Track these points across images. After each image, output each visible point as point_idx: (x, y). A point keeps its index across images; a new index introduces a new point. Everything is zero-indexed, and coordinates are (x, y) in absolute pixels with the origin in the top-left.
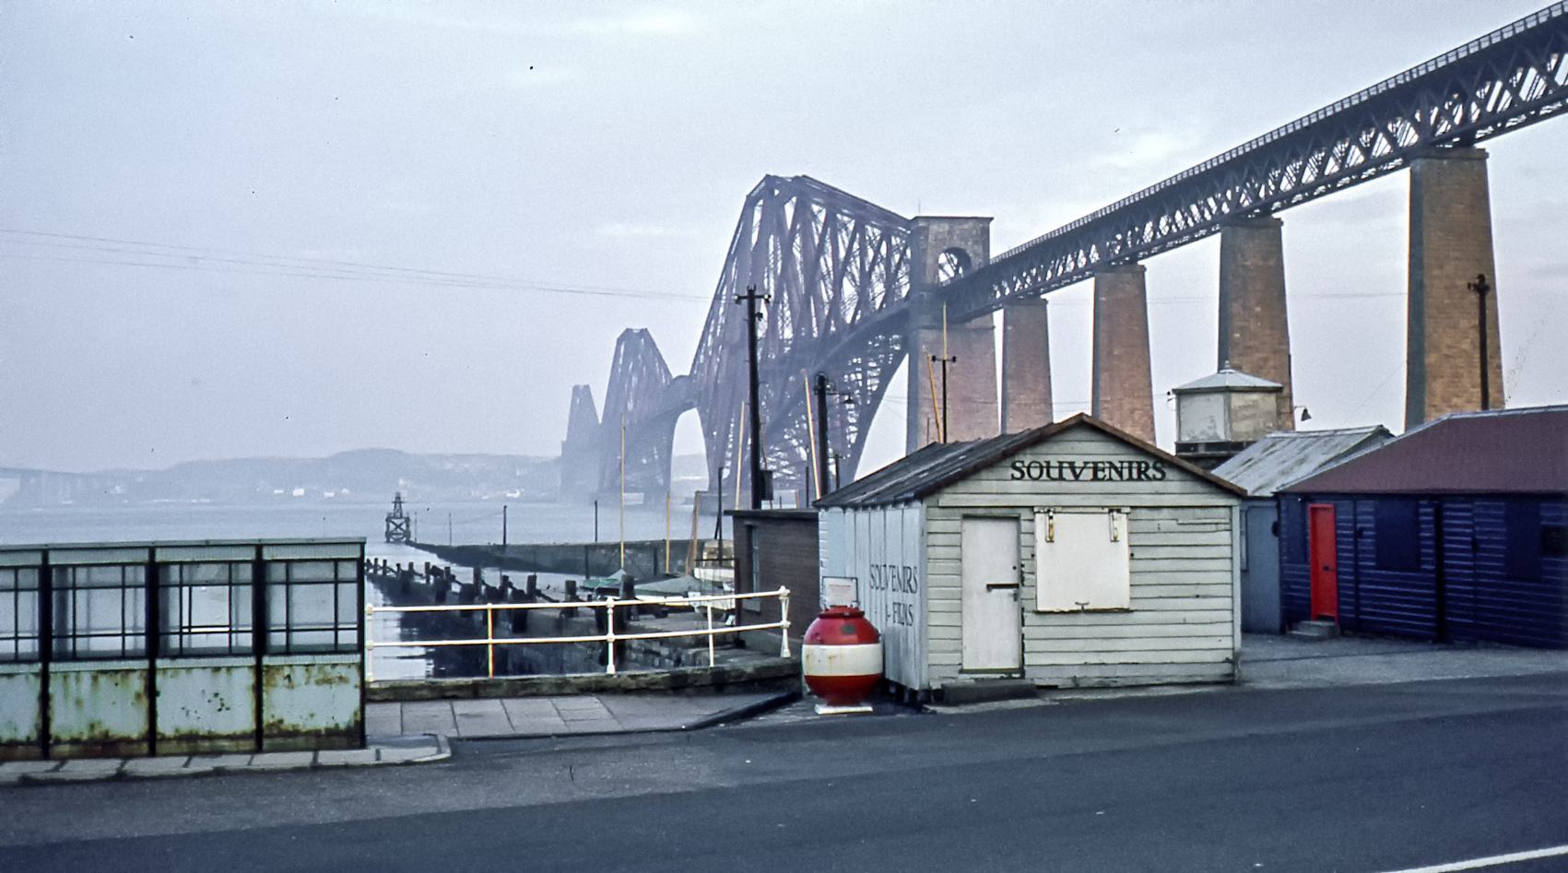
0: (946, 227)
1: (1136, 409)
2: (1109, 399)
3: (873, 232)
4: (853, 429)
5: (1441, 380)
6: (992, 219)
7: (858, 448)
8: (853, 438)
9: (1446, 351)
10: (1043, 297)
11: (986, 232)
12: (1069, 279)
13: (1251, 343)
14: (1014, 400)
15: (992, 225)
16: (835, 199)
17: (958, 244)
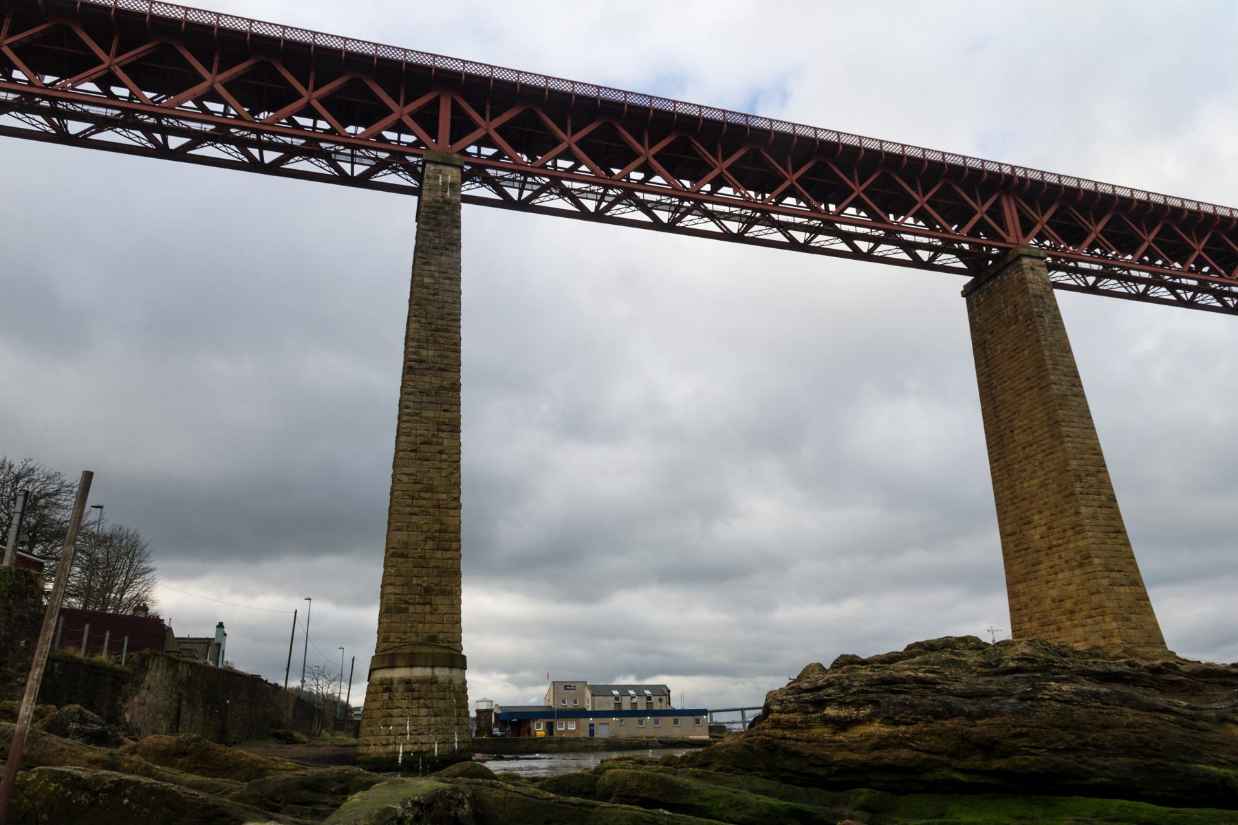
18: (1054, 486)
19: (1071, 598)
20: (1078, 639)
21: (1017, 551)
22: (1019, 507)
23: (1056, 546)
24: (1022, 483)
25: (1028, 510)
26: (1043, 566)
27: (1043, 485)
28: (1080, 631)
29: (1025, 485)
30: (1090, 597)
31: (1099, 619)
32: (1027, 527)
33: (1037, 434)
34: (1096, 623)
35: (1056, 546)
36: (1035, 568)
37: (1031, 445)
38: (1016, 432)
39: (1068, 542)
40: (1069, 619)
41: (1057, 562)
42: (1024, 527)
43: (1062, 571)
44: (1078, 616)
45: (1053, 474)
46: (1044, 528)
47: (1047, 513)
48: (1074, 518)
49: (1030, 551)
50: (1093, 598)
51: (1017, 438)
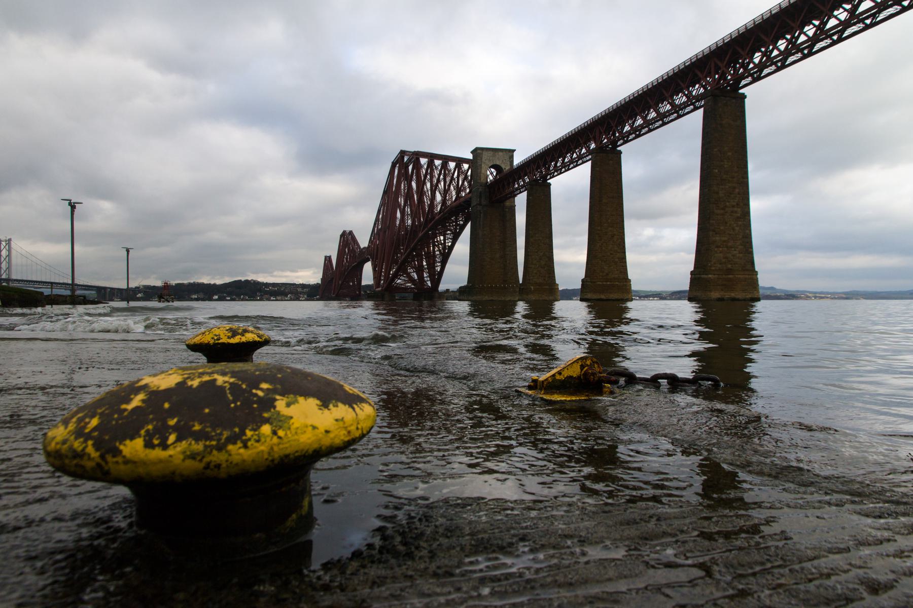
0: (490, 153)
1: (614, 235)
2: (599, 228)
3: (452, 165)
4: (439, 264)
6: (515, 150)
7: (441, 273)
8: (438, 269)
10: (548, 181)
11: (512, 157)
12: (566, 167)
13: (724, 176)
15: (515, 153)
16: (432, 157)
17: (498, 163)
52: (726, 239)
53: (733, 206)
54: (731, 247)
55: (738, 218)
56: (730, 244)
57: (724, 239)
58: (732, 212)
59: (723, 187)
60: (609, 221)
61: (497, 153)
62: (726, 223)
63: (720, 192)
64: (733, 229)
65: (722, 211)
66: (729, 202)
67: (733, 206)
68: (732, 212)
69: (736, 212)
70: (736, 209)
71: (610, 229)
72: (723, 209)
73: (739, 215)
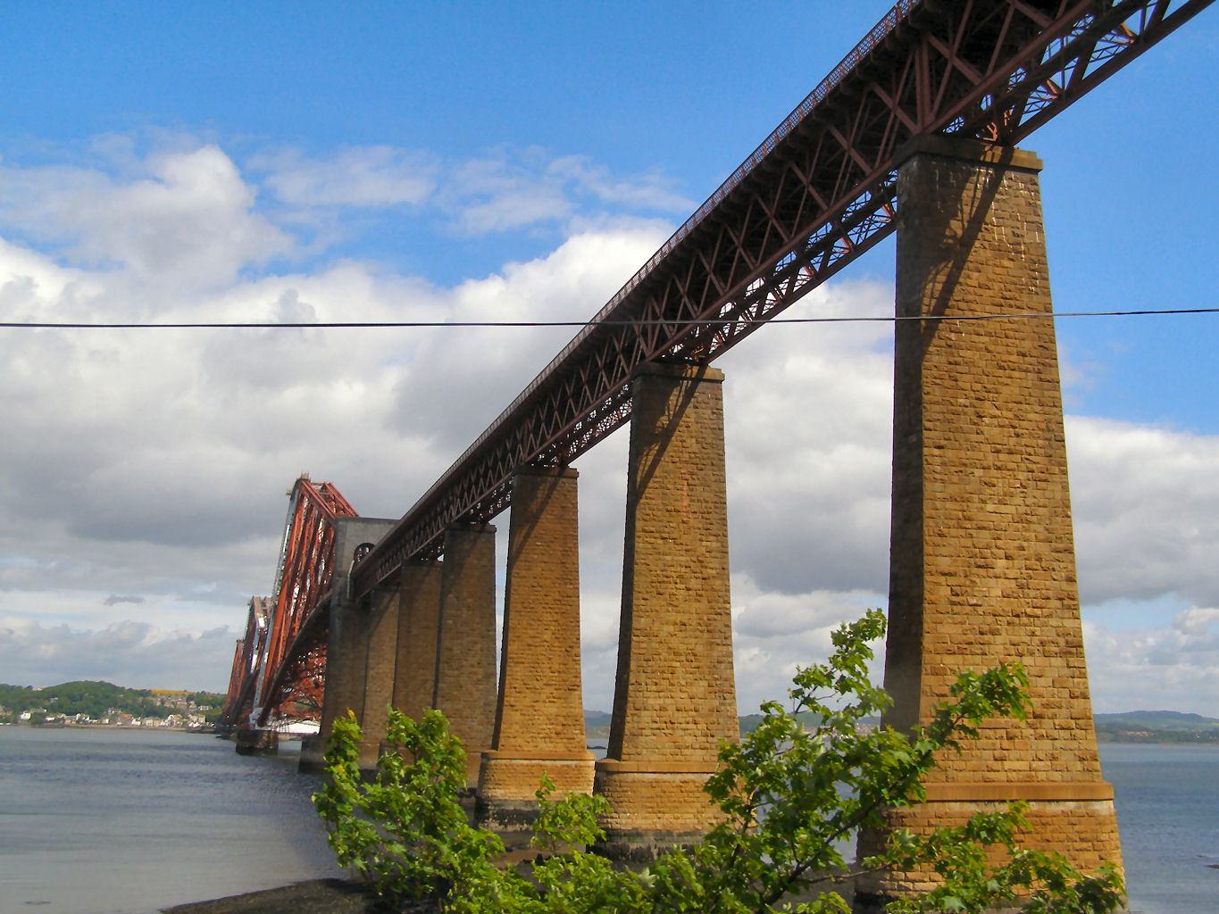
1: (427, 680)
5: (521, 665)
9: (530, 641)
14: (373, 668)
18: (1040, 528)
19: (1041, 696)
20: (1041, 755)
21: (953, 603)
22: (971, 536)
23: (1029, 616)
24: (984, 502)
25: (988, 547)
26: (998, 638)
27: (1023, 520)
28: (1047, 744)
29: (990, 507)
30: (1072, 701)
31: (1078, 732)
32: (981, 571)
33: (1024, 441)
34: (1074, 738)
35: (1029, 616)
36: (986, 638)
37: (1011, 453)
38: (986, 420)
39: (1050, 616)
40: (1031, 726)
41: (1027, 639)
42: (975, 570)
43: (1032, 654)
44: (1047, 723)
45: (1041, 511)
46: (1013, 584)
47: (1019, 563)
48: (1065, 585)
49: (980, 610)
50: (1075, 701)
51: (985, 429)
52: (461, 706)
53: (473, 666)
54: (467, 717)
55: (479, 680)
56: (465, 713)
57: (456, 707)
58: (471, 673)
59: (459, 641)
60: (421, 660)
61: (369, 526)
62: (461, 687)
63: (455, 648)
64: (471, 694)
65: (456, 672)
66: (466, 660)
67: (473, 666)
68: (471, 673)
69: (475, 673)
70: (474, 670)
71: (421, 671)
72: (457, 669)
73: (480, 677)
